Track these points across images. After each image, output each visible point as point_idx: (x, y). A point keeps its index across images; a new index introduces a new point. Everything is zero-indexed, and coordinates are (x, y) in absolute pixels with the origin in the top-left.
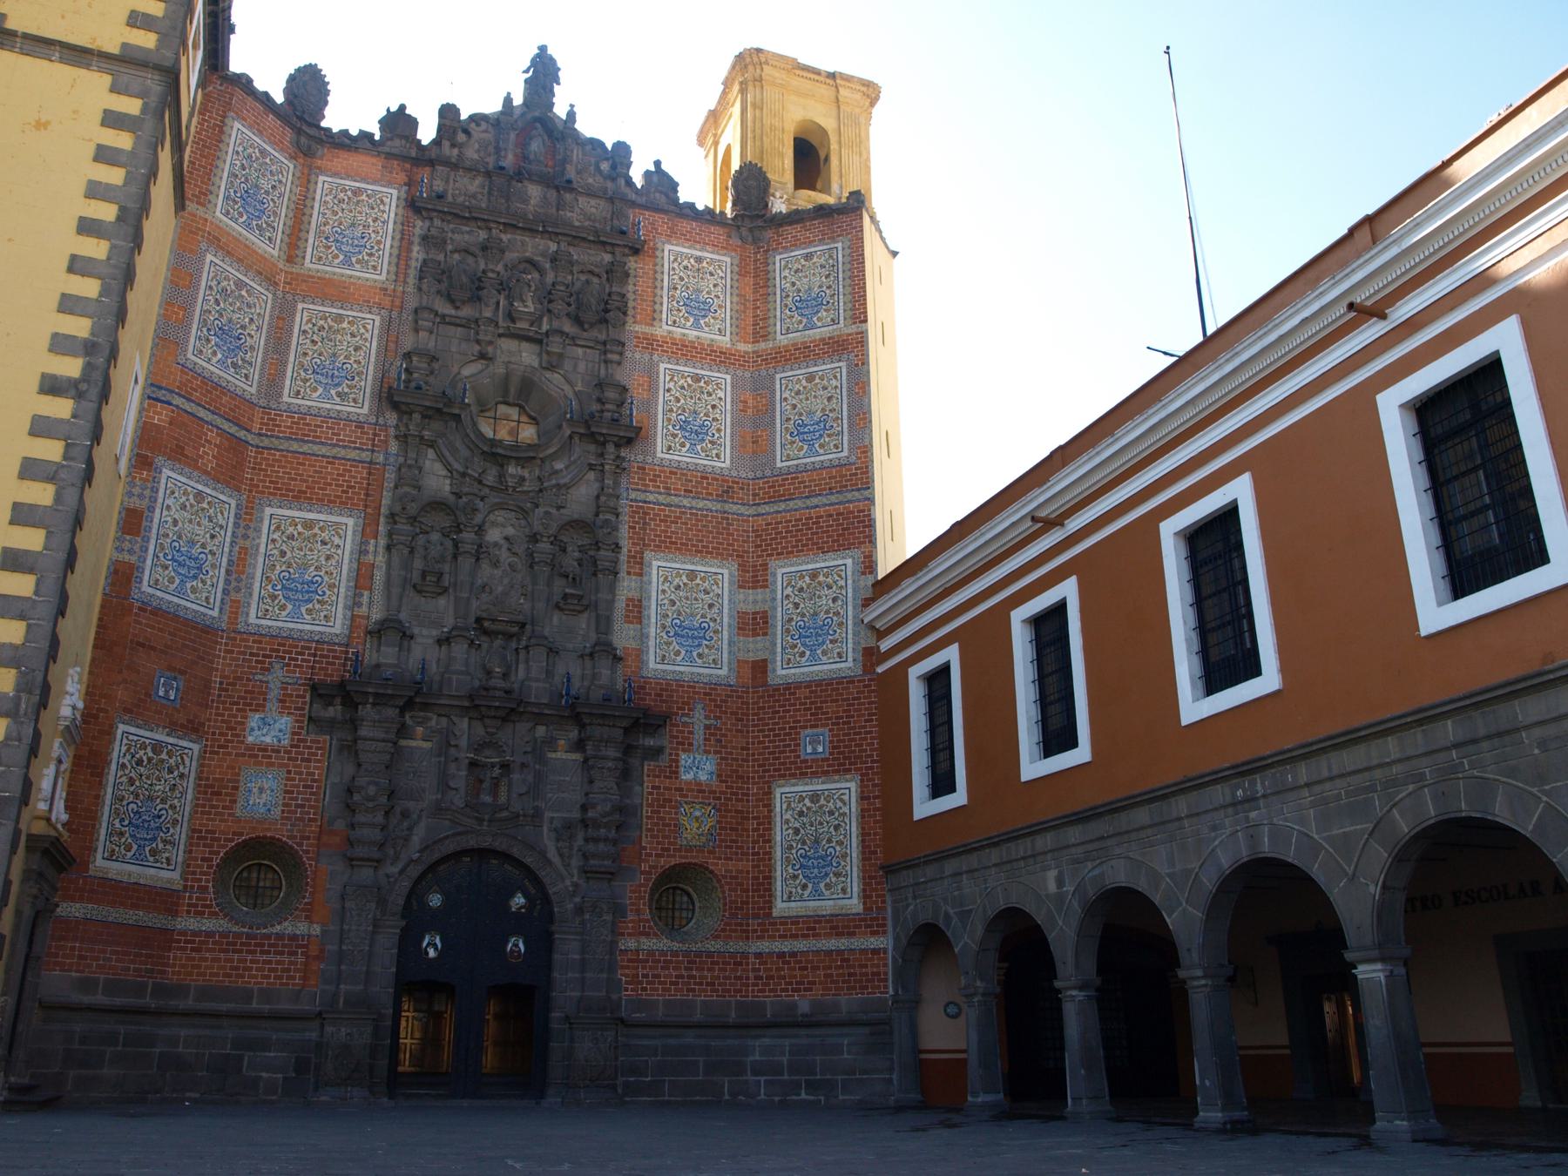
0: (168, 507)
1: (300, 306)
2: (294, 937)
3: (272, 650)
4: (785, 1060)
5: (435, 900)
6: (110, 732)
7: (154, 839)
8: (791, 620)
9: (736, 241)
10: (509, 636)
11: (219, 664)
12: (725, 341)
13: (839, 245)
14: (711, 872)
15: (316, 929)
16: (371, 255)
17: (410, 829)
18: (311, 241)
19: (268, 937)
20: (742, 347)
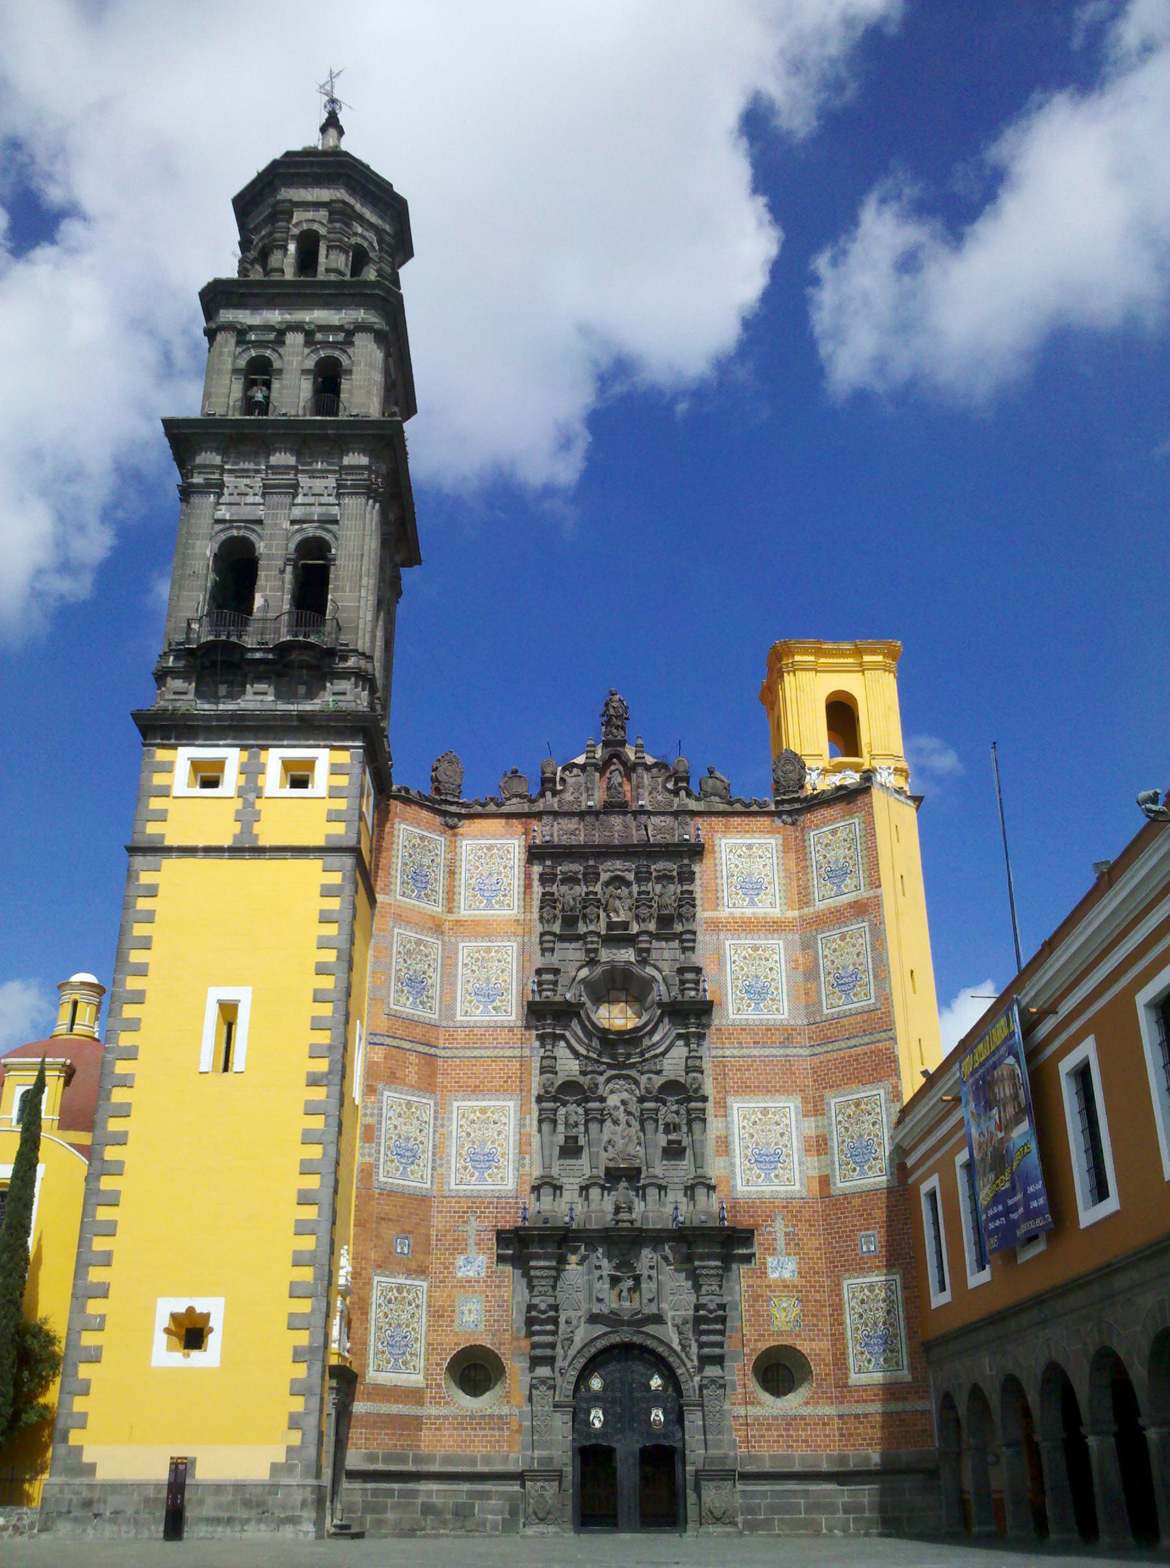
0: (390, 1118)
1: (461, 945)
2: (500, 1417)
3: (469, 1207)
5: (596, 1384)
6: (368, 1283)
7: (404, 1353)
8: (843, 1141)
12: (776, 912)
13: (856, 820)
16: (505, 895)
19: (483, 1417)
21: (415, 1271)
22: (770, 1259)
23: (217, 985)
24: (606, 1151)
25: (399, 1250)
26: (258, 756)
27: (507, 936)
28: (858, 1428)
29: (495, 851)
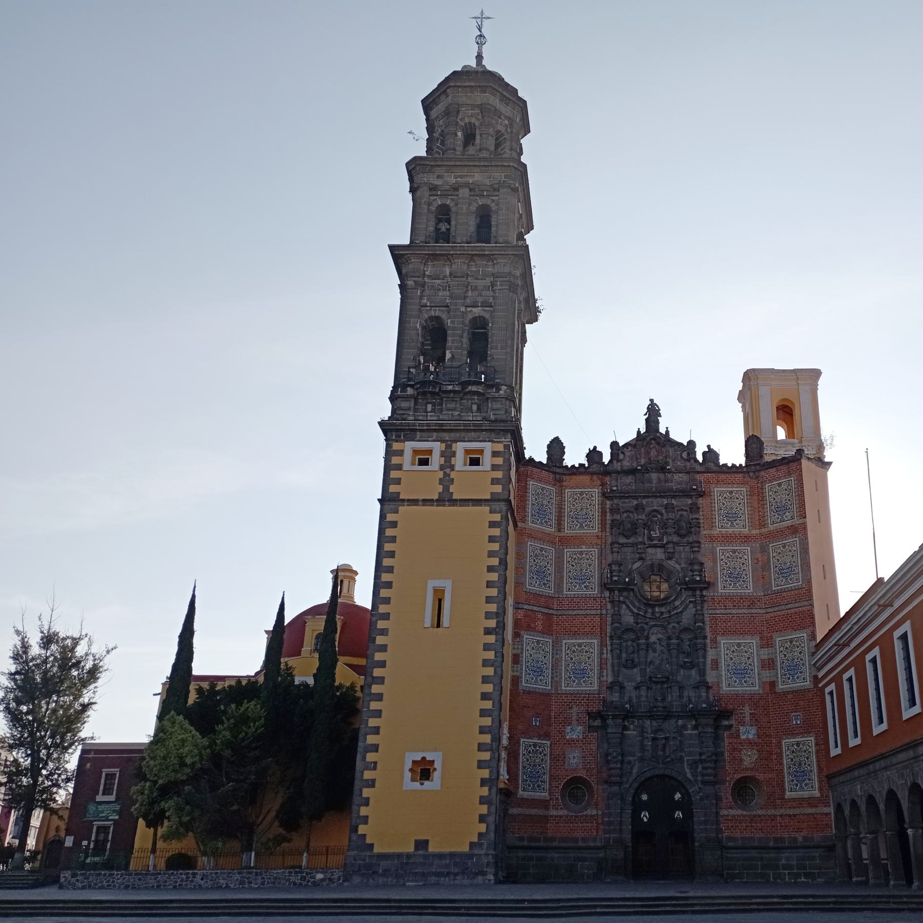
10: (663, 683)
12: (746, 531)
17: (632, 768)
20: (754, 532)
22: (741, 728)
27: (592, 545)
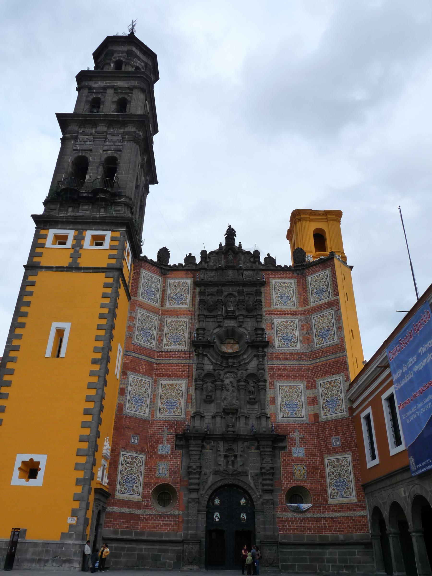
0: (132, 386)
1: (166, 319)
2: (174, 515)
4: (337, 557)
5: (217, 502)
6: (118, 455)
7: (133, 486)
8: (324, 399)
9: (295, 274)
11: (149, 430)
12: (295, 308)
13: (328, 271)
14: (306, 489)
15: (181, 513)
16: (185, 300)
18: (167, 299)
19: (167, 515)
20: (301, 309)
21: (140, 451)
22: (293, 449)
23: (56, 321)
24: (223, 402)
25: (133, 441)
26: (81, 233)
28: (332, 523)
29: (181, 284)
